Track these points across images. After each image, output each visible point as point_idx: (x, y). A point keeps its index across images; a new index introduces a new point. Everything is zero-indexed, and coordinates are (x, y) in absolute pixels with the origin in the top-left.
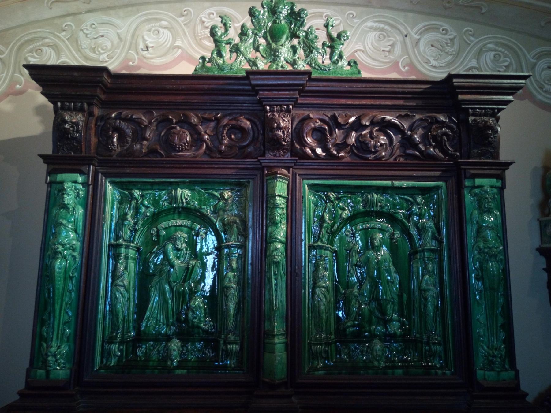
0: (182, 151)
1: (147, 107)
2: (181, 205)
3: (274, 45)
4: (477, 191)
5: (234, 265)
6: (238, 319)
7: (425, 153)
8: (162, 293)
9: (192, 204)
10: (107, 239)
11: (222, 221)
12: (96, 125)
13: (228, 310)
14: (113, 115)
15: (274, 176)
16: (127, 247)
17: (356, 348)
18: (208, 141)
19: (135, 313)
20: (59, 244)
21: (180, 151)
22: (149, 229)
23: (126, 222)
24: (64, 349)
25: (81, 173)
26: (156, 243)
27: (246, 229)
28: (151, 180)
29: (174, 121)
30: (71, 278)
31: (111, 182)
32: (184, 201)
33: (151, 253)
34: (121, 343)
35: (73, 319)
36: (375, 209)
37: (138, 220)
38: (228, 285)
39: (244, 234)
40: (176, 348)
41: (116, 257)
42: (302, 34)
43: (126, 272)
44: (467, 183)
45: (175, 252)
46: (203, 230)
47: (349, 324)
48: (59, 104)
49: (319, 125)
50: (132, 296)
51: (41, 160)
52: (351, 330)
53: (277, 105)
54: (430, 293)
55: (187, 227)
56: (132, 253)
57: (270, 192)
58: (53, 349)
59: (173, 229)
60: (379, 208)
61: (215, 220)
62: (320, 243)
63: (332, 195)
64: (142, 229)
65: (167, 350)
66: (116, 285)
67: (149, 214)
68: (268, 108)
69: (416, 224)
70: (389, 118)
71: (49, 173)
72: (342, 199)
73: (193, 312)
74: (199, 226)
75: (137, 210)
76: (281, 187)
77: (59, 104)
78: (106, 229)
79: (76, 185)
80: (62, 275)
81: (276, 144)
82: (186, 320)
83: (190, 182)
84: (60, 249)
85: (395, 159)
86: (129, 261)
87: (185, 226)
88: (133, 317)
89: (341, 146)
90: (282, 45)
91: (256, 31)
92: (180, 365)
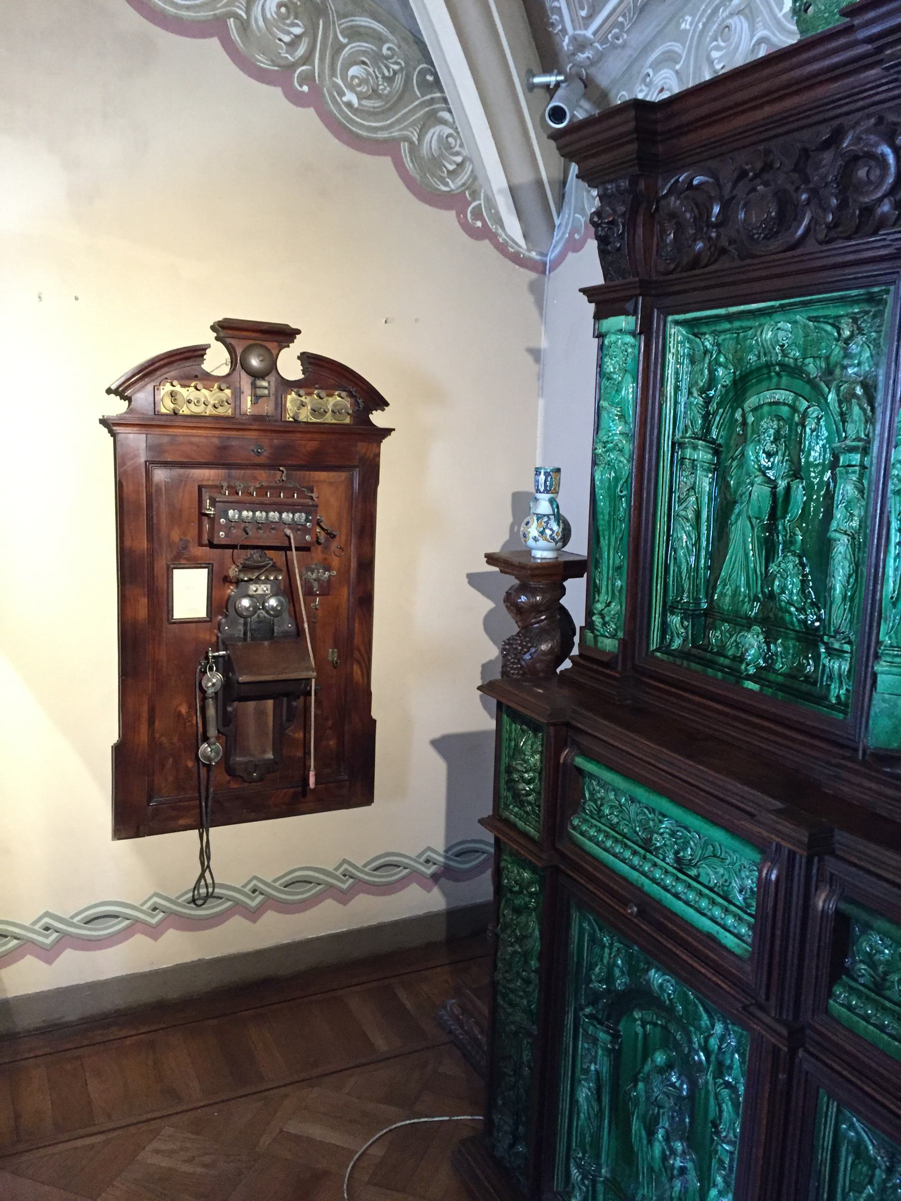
9: (791, 355)
19: (709, 568)
22: (734, 411)
25: (626, 313)
28: (722, 311)
31: (677, 323)
51: (585, 298)
55: (788, 405)
58: (599, 606)
64: (721, 411)
71: (599, 316)
74: (806, 404)
82: (772, 596)
83: (782, 306)
87: (784, 404)
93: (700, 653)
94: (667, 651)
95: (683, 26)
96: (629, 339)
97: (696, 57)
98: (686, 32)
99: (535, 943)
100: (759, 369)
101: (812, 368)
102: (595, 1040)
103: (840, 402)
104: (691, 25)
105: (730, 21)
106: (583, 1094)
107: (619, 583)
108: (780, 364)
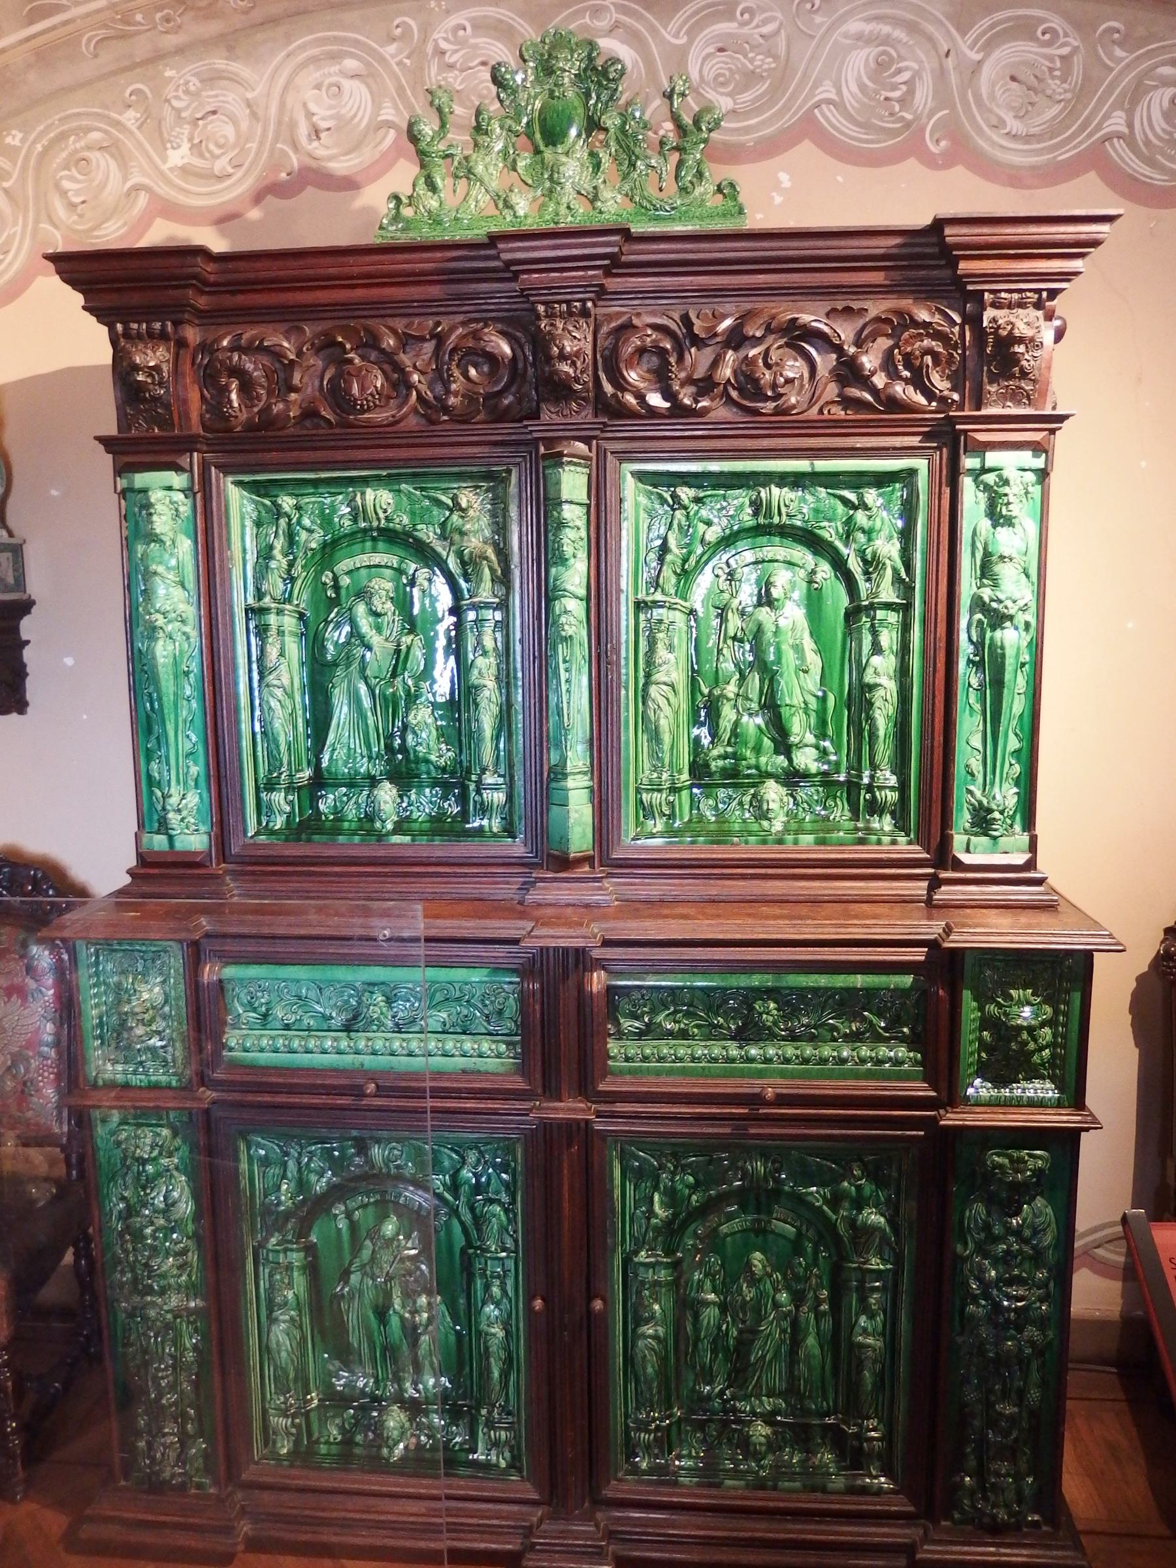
0: (369, 410)
1: (291, 317)
2: (375, 524)
3: (548, 154)
4: (990, 478)
5: (488, 643)
6: (502, 746)
7: (882, 396)
8: (355, 699)
10: (240, 596)
11: (460, 554)
12: (193, 363)
13: (480, 729)
14: (225, 343)
15: (557, 459)
16: (280, 612)
17: (730, 797)
18: (420, 386)
20: (158, 611)
21: (363, 412)
23: (273, 564)
24: (193, 799)
25: (178, 468)
26: (331, 601)
27: (507, 571)
29: (348, 346)
30: (187, 674)
31: (238, 484)
32: (382, 515)
33: (327, 623)
34: (289, 789)
35: (201, 749)
36: (776, 520)
37: (295, 559)
38: (476, 682)
39: (504, 579)
40: (387, 798)
41: (262, 631)
42: (611, 121)
43: (282, 660)
44: (970, 462)
45: (371, 619)
46: (423, 574)
47: (715, 753)
48: (119, 327)
49: (653, 341)
50: (299, 706)
51: (102, 447)
52: (720, 763)
53: (560, 302)
54: (880, 692)
55: (391, 568)
56: (290, 622)
57: (552, 495)
58: (174, 801)
59: (363, 572)
60: (784, 518)
61: (444, 554)
62: (658, 596)
63: (686, 493)
65: (371, 800)
66: (268, 686)
67: (314, 545)
68: (541, 308)
69: (861, 553)
70: (805, 318)
71: (120, 470)
72: (707, 500)
73: (415, 733)
74: (413, 566)
75: (291, 538)
76: (573, 483)
77: (119, 327)
78: (236, 574)
79: (172, 493)
80: (170, 670)
81: (559, 391)
82: (403, 749)
83: (389, 476)
84: (160, 621)
85: (821, 412)
86: (287, 639)
87: (387, 567)
88: (304, 744)
89: (706, 385)
90: (567, 154)
91: (509, 122)
92: (399, 829)
93: (307, 826)
94: (272, 832)
95: (9, 140)
96: (181, 496)
97: (37, 179)
98: (16, 150)
99: (186, 1207)
100: (353, 534)
101: (428, 534)
102: (289, 1268)
103: (463, 563)
104: (23, 141)
105: (94, 156)
106: (280, 1335)
107: (194, 770)
108: (379, 529)
